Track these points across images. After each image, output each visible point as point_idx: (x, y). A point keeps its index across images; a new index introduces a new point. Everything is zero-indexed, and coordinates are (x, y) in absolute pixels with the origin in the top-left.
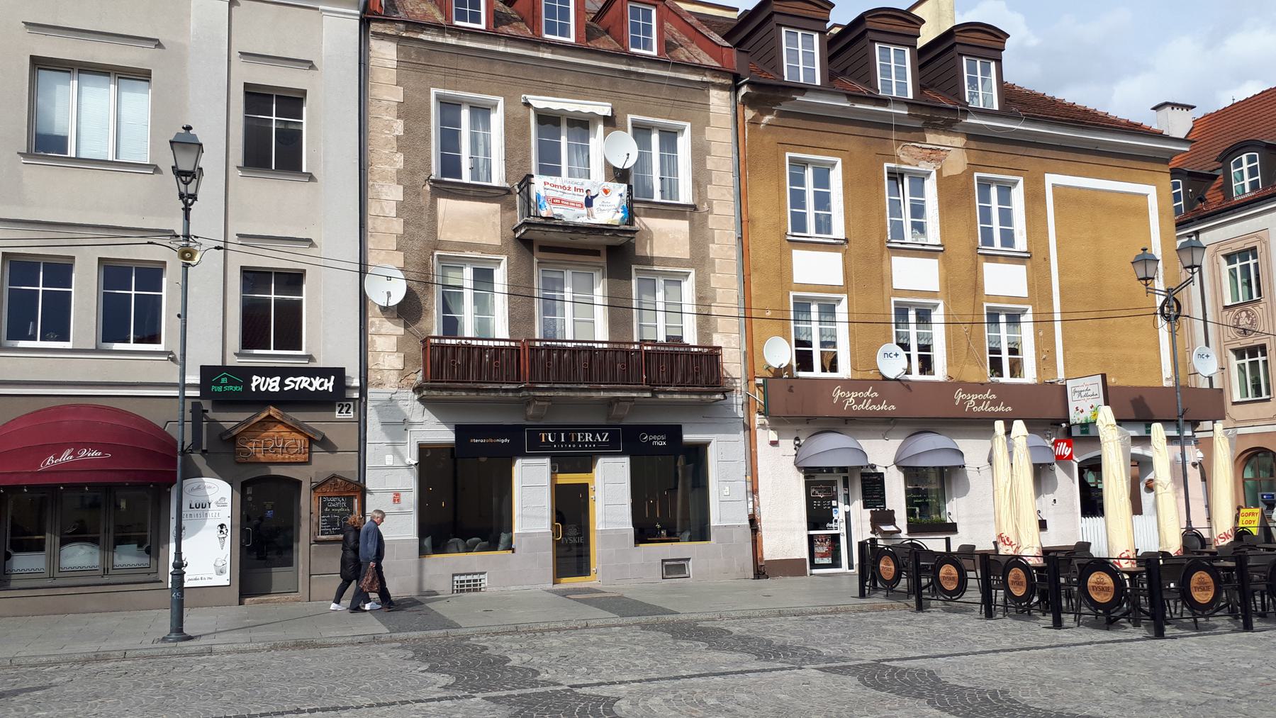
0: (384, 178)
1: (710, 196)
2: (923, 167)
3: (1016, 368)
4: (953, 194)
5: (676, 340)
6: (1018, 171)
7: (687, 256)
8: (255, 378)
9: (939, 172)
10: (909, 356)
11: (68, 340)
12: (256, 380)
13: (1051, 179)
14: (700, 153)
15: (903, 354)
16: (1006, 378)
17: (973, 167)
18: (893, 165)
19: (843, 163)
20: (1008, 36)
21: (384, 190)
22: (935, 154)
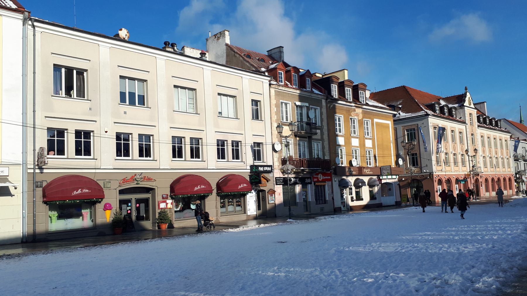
0: (274, 121)
1: (323, 125)
2: (356, 117)
3: (370, 164)
4: (361, 123)
5: (318, 158)
6: (370, 118)
7: (320, 138)
8: (259, 167)
9: (358, 119)
10: (357, 161)
11: (225, 159)
12: (260, 168)
13: (376, 120)
14: (321, 114)
15: (356, 160)
16: (369, 166)
17: (363, 117)
18: (351, 117)
19: (344, 117)
20: (367, 86)
21: (274, 124)
22: (357, 115)
